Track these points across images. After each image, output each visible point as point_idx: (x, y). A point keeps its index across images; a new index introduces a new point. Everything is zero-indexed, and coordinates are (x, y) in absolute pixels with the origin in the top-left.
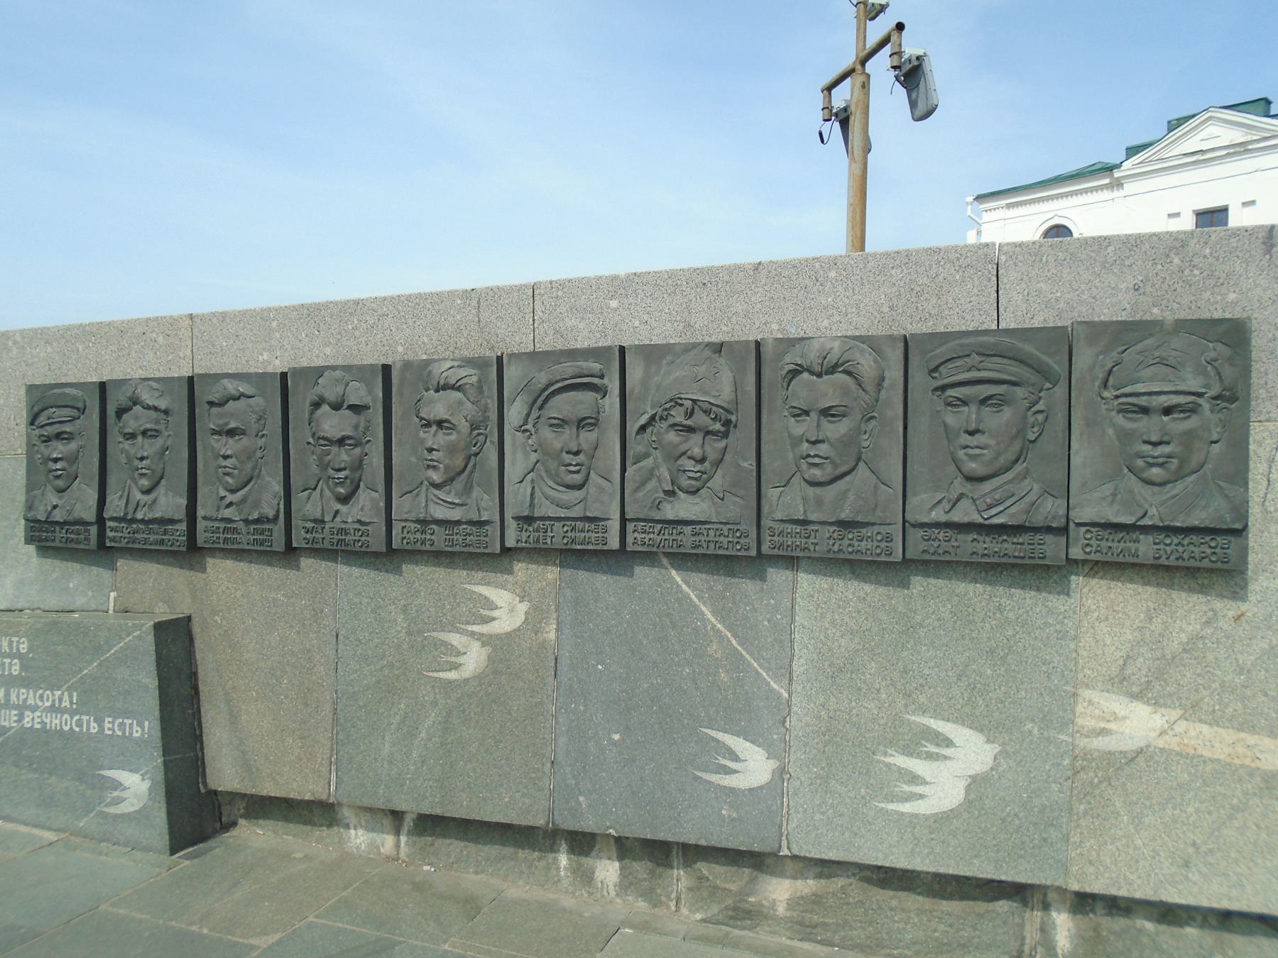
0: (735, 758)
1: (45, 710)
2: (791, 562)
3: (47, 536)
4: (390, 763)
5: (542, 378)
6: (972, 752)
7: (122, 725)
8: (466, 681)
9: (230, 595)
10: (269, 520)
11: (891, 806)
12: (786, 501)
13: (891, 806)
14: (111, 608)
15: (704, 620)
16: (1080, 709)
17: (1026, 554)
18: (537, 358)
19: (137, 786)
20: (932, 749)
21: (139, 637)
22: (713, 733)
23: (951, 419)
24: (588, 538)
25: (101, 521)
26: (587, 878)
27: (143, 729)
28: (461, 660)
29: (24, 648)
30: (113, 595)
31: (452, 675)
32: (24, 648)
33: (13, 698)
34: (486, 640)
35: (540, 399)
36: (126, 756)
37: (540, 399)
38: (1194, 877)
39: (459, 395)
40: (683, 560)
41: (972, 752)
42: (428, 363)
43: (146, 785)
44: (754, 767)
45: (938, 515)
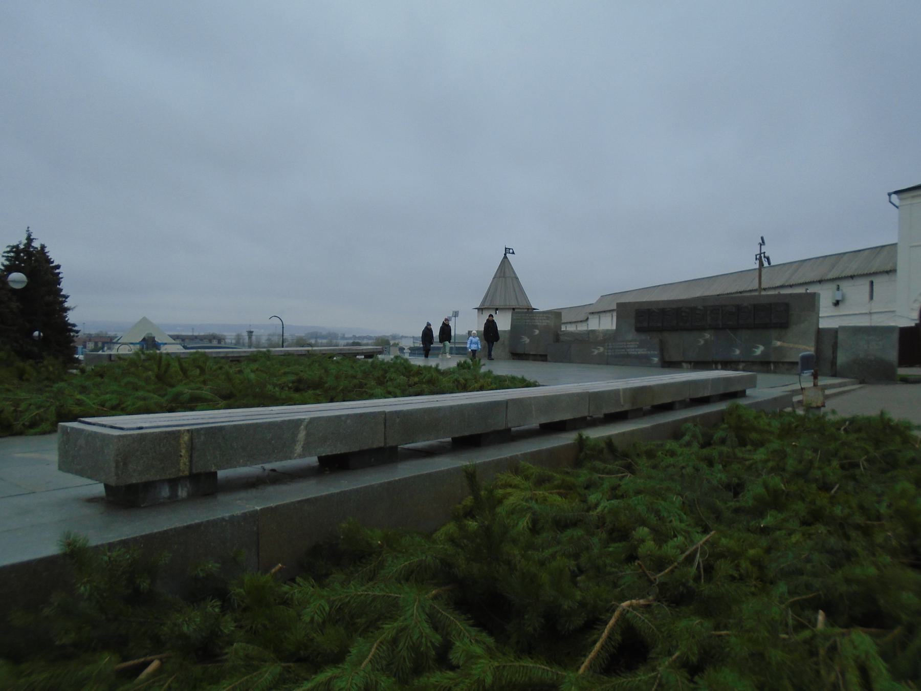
1: (641, 352)
3: (639, 330)
17: (766, 327)
36: (655, 356)
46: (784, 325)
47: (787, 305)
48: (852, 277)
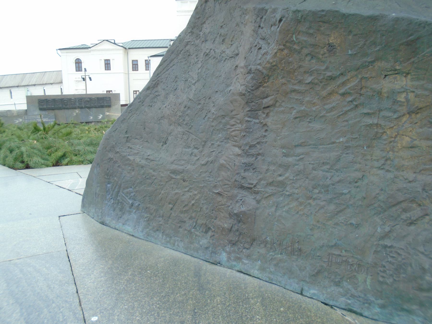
3: (41, 109)
6: (101, 116)
17: (102, 107)
35: (79, 100)
37: (79, 100)
41: (101, 116)
44: (92, 118)
46: (109, 106)
48: (34, 85)
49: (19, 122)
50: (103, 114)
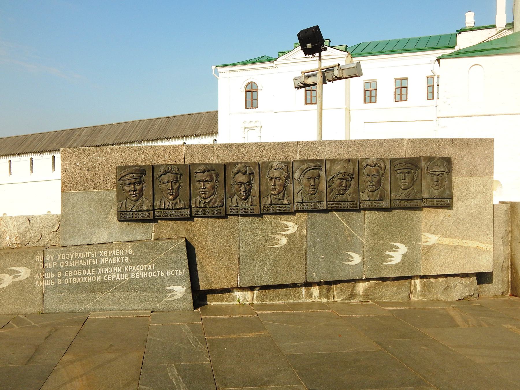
0: (352, 258)
1: (139, 272)
2: (363, 209)
3: (124, 217)
4: (258, 273)
5: (305, 166)
6: (403, 249)
7: (174, 272)
8: (281, 247)
9: (201, 230)
10: (220, 206)
11: (387, 263)
12: (364, 196)
13: (387, 263)
14: (153, 239)
15: (344, 225)
16: (423, 237)
17: (414, 205)
18: (303, 162)
19: (181, 291)
20: (395, 249)
21: (180, 244)
22: (347, 252)
23: (398, 176)
24: (319, 206)
25: (154, 210)
26: (310, 295)
27: (183, 272)
28: (279, 242)
29: (130, 252)
30: (153, 234)
31: (277, 246)
32: (130, 252)
33: (126, 269)
34: (286, 236)
36: (176, 281)
38: (443, 269)
39: (282, 171)
40: (336, 211)
41: (403, 249)
42: (270, 162)
43: (185, 289)
45: (397, 198)
47: (448, 161)
49: (14, 285)
50: (411, 238)
